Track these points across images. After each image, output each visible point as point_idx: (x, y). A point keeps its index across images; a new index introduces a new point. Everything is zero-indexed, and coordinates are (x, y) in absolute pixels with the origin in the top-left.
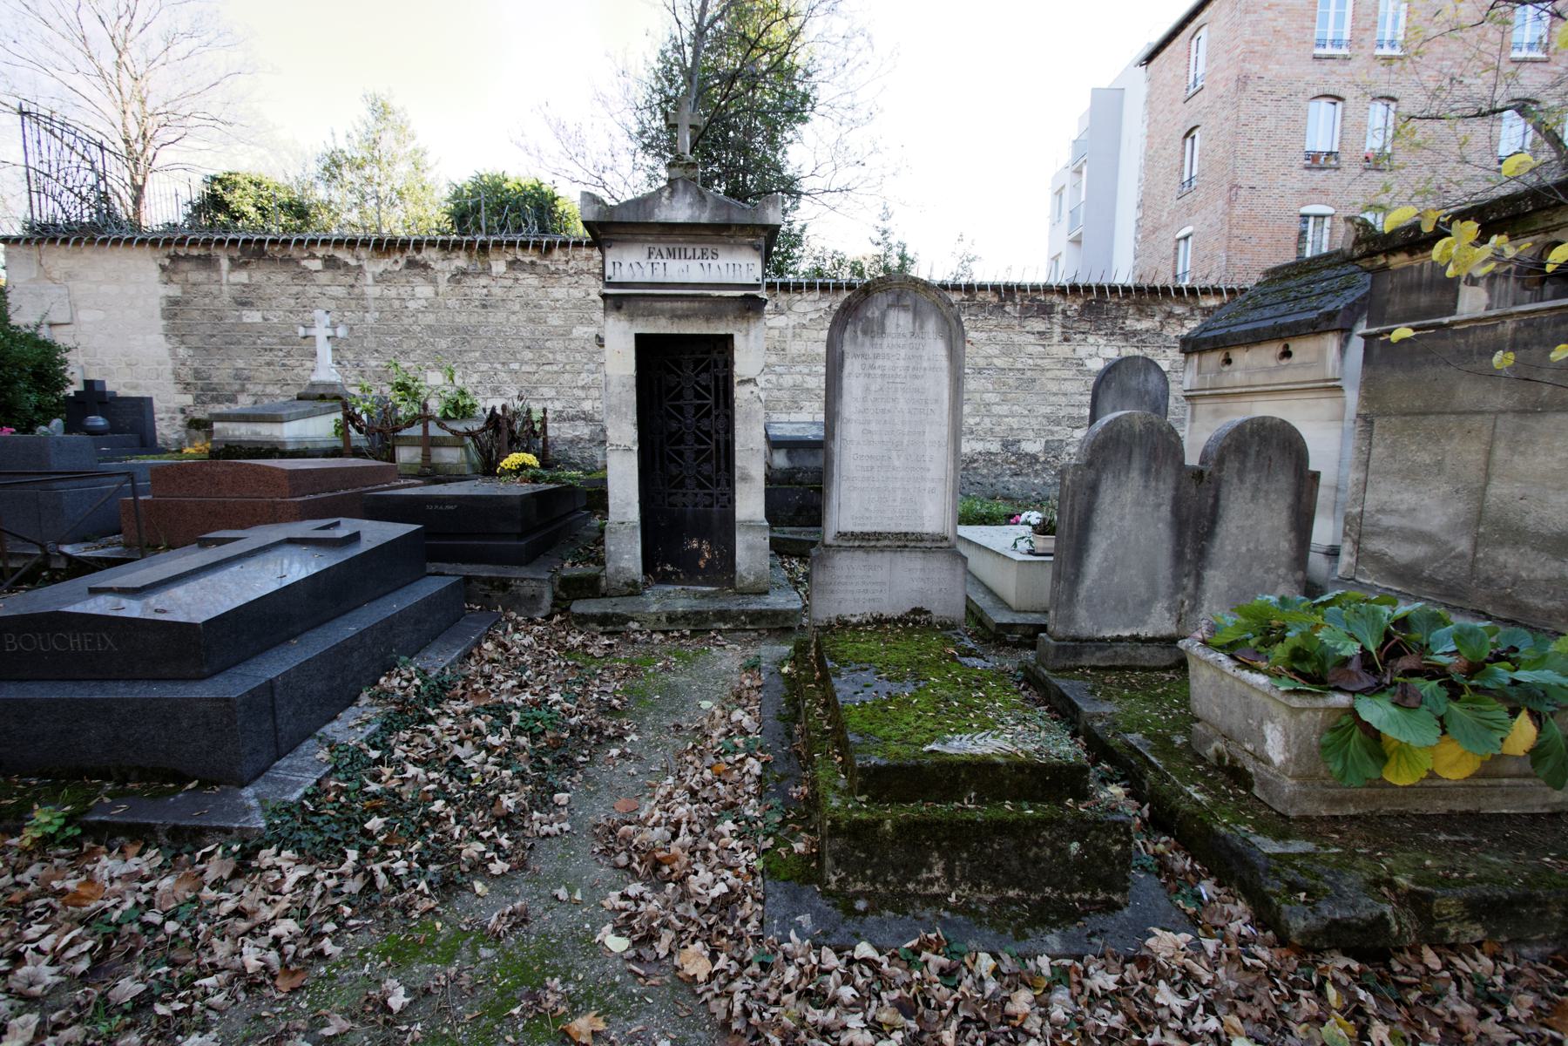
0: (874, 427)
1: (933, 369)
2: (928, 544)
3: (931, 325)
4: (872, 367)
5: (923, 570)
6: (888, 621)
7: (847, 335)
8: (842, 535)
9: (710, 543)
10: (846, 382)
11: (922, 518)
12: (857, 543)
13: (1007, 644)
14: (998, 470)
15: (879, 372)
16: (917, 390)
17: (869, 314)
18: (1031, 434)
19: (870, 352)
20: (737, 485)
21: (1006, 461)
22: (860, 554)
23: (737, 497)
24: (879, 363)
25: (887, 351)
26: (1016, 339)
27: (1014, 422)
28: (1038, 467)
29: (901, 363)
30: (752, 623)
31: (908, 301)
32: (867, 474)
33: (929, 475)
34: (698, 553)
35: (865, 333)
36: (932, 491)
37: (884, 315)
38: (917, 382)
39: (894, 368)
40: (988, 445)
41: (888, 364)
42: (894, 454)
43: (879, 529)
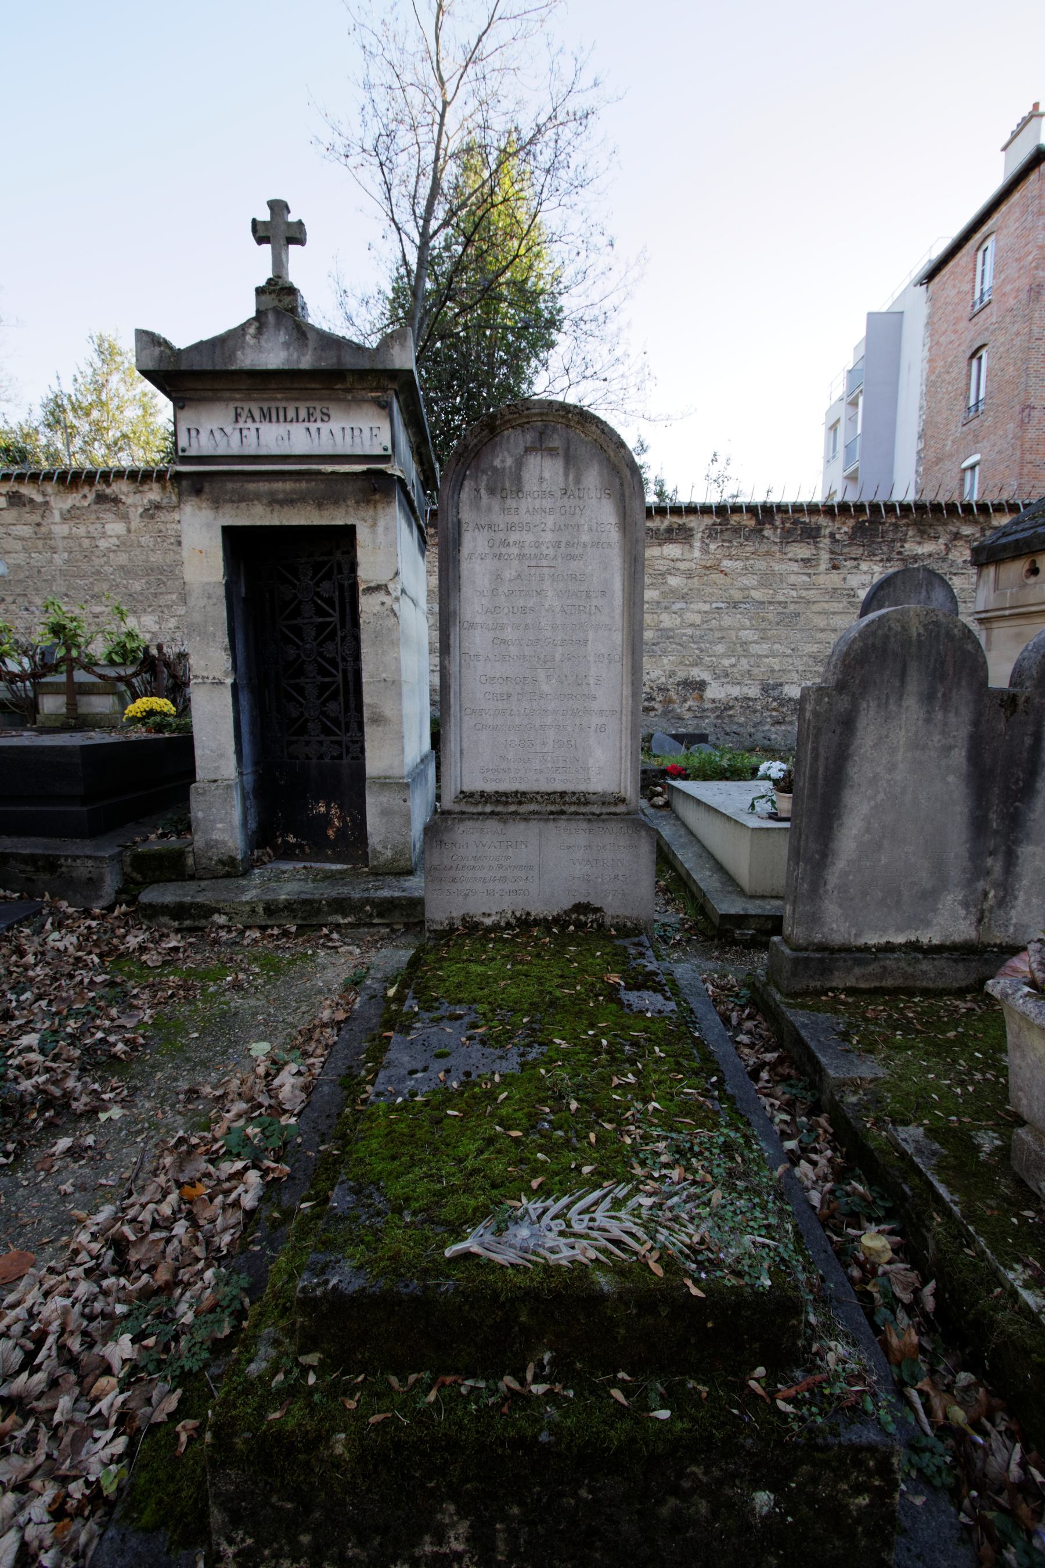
0: (509, 634)
1: (596, 545)
3: (593, 477)
4: (505, 543)
5: (589, 847)
6: (537, 922)
7: (465, 495)
8: (466, 796)
9: (340, 807)
10: (465, 567)
11: (586, 769)
12: (488, 809)
13: (735, 942)
14: (756, 717)
15: (514, 550)
16: (574, 578)
17: (497, 463)
18: (795, 677)
19: (500, 520)
20: (366, 729)
21: (766, 707)
22: (492, 824)
23: (367, 745)
24: (514, 537)
25: (526, 518)
26: (776, 567)
27: (775, 663)
29: (548, 537)
30: (380, 915)
31: (556, 442)
32: (500, 705)
33: (595, 706)
34: (325, 820)
35: (492, 491)
36: (601, 729)
37: (519, 464)
38: (574, 565)
39: (538, 545)
40: (745, 690)
41: (529, 538)
42: (541, 675)
43: (522, 787)
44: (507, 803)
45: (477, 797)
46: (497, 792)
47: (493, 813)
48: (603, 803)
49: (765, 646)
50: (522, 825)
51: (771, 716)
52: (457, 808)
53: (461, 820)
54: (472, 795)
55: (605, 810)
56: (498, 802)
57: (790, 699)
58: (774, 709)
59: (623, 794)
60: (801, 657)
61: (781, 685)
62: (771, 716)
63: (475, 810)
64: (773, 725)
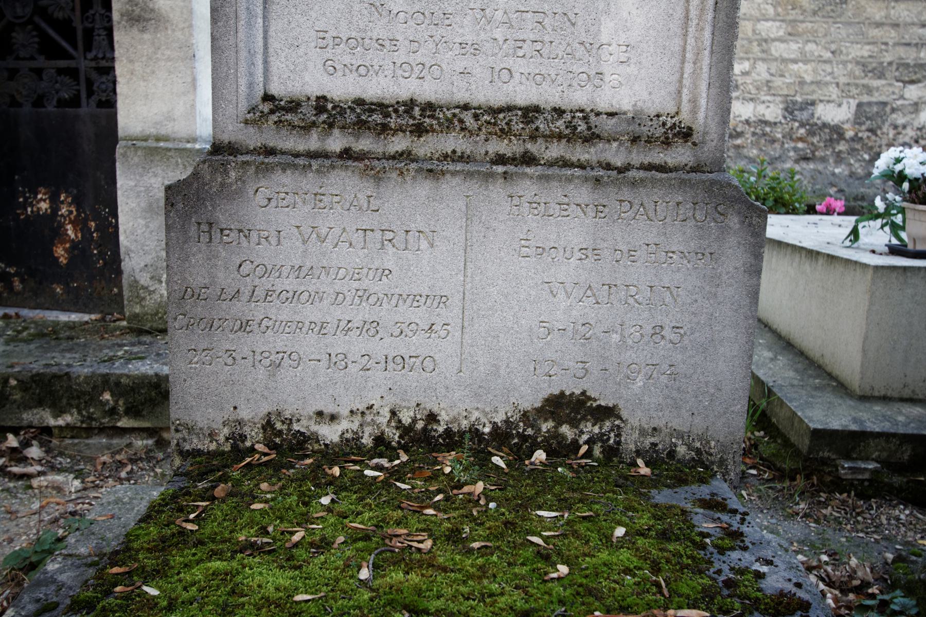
2: (615, 154)
5: (591, 252)
6: (452, 440)
9: (78, 202)
11: (592, 47)
12: (336, 143)
13: (839, 485)
14: (774, 151)
18: (834, 92)
20: (117, 36)
21: (789, 136)
22: (345, 183)
23: (120, 69)
27: (806, 71)
28: (842, 147)
30: (133, 411)
34: (50, 227)
40: (761, 109)
43: (427, 90)
44: (384, 129)
45: (308, 111)
46: (360, 102)
47: (347, 154)
48: (635, 140)
49: (794, 46)
50: (423, 189)
51: (795, 149)
52: (252, 138)
53: (264, 170)
54: (294, 105)
55: (638, 157)
56: (361, 125)
57: (825, 125)
58: (801, 139)
59: (685, 117)
60: (844, 63)
61: (813, 103)
62: (795, 149)
63: (301, 147)
64: (797, 161)
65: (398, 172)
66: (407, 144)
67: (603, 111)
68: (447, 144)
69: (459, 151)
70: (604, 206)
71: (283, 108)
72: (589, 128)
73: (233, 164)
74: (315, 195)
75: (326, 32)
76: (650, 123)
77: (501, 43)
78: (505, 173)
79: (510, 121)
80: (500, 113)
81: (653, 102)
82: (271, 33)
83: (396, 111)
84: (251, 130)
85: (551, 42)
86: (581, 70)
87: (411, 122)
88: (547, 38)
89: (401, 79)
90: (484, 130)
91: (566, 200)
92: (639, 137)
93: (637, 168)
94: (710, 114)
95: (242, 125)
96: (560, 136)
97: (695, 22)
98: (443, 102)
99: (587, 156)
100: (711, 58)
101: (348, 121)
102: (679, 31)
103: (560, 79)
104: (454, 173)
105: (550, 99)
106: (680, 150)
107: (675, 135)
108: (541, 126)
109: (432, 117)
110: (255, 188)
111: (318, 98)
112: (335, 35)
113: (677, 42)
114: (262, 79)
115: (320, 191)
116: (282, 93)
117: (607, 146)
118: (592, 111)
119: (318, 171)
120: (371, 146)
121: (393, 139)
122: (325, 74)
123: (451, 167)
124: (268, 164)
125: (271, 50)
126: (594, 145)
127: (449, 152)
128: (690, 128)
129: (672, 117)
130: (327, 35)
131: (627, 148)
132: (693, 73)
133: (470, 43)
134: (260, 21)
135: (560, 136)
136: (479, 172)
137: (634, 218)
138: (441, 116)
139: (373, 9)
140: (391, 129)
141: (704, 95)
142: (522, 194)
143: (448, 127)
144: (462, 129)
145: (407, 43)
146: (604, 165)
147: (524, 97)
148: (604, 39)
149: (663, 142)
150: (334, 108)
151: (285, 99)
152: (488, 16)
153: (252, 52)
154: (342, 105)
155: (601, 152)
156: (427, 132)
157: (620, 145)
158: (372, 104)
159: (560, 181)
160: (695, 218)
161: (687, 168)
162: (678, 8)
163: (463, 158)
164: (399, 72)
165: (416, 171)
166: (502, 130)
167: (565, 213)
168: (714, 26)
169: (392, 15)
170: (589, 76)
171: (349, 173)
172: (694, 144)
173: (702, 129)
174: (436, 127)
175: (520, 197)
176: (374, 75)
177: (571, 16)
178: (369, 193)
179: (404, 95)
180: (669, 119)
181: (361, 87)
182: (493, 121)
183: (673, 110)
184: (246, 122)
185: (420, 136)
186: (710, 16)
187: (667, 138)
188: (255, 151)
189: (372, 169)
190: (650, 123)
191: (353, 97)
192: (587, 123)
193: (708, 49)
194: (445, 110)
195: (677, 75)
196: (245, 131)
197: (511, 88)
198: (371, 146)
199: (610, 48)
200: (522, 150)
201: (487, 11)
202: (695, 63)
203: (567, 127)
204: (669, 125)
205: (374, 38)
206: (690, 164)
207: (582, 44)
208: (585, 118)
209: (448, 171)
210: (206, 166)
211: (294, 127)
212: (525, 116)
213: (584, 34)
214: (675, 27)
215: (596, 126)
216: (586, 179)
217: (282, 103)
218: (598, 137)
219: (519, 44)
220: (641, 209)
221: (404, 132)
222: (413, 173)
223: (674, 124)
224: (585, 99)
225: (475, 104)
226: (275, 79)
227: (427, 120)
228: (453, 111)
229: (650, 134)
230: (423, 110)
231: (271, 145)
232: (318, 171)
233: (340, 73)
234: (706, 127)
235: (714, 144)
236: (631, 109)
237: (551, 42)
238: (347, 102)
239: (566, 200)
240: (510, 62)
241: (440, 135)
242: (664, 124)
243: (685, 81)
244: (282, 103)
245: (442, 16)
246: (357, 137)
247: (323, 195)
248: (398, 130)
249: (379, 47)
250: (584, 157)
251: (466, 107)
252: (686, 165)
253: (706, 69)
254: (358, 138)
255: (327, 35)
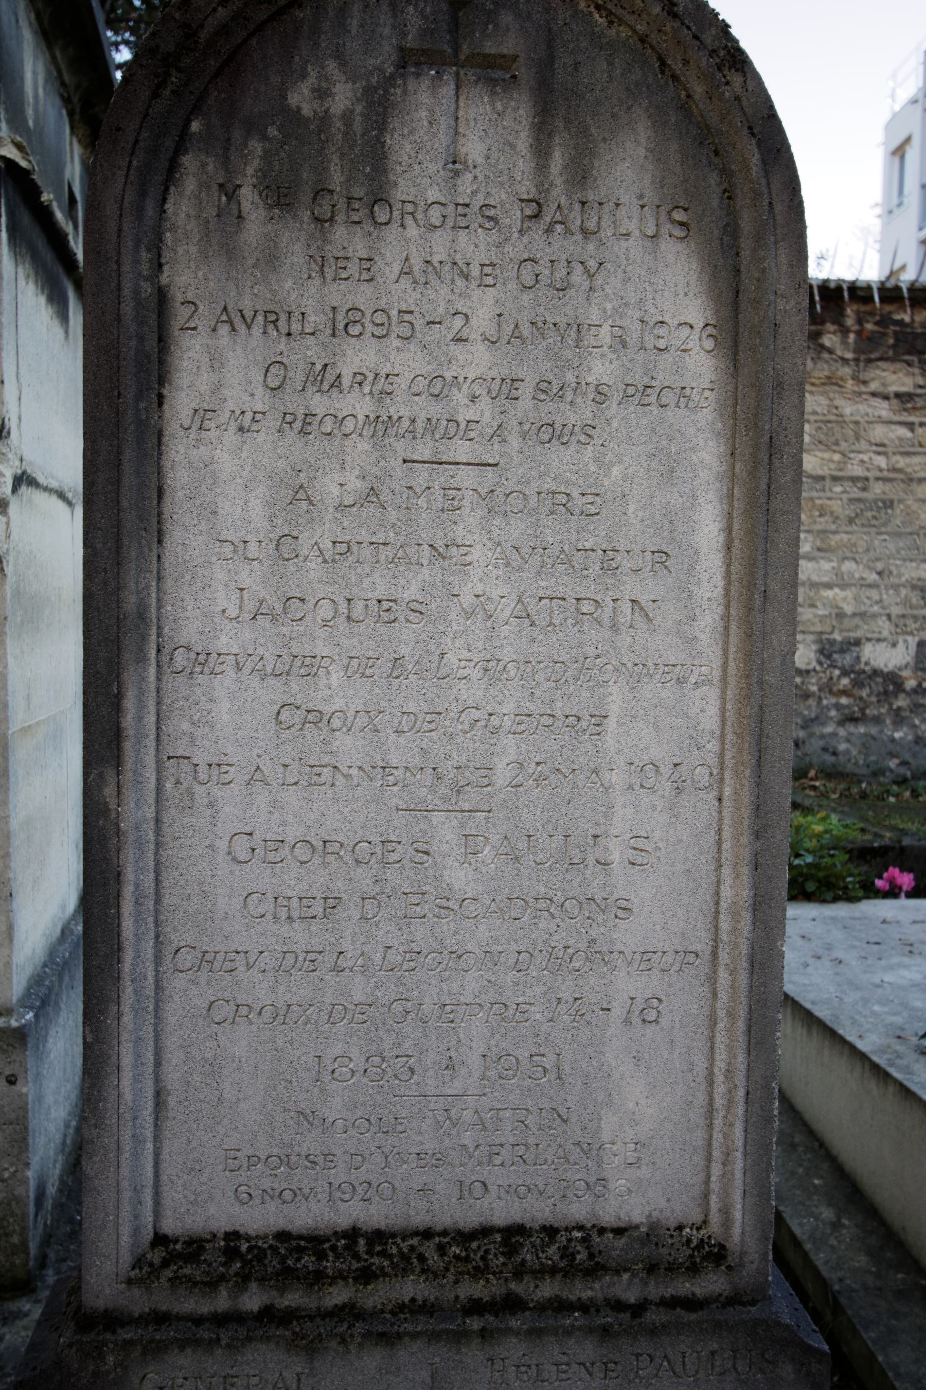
0: (335, 691)
1: (641, 393)
2: (627, 1289)
3: (629, 169)
4: (324, 379)
7: (182, 207)
8: (174, 1255)
10: (182, 457)
11: (592, 1150)
12: (252, 1300)
14: (809, 709)
15: (359, 405)
16: (560, 504)
17: (301, 98)
18: (885, 628)
19: (311, 298)
21: (828, 688)
24: (356, 357)
25: (402, 295)
26: (848, 409)
27: (845, 599)
28: (901, 702)
29: (477, 361)
31: (508, 40)
32: (301, 937)
33: (628, 936)
35: (280, 197)
36: (645, 1014)
37: (380, 107)
38: (560, 459)
39: (438, 387)
41: (408, 363)
42: (445, 831)
44: (318, 1278)
45: (213, 1255)
46: (283, 1236)
47: (267, 1314)
48: (651, 1268)
49: (826, 566)
50: (372, 1360)
51: (838, 706)
52: (138, 1302)
53: (155, 1350)
54: (194, 1247)
55: (656, 1290)
56: (287, 1276)
57: (876, 672)
58: (844, 693)
59: (715, 1226)
60: (896, 587)
61: (857, 643)
62: (838, 706)
63: (205, 1308)
64: (841, 723)
65: (339, 1339)
66: (349, 1295)
67: (608, 1225)
68: (404, 1292)
69: (419, 1298)
70: (616, 1363)
71: (180, 1256)
72: (591, 1256)
73: (111, 1346)
74: (225, 1377)
75: (238, 1150)
76: (670, 1241)
77: (471, 1150)
78: (483, 1329)
79: (487, 1252)
80: (473, 1240)
81: (673, 1211)
82: (165, 1155)
83: (334, 1248)
84: (136, 1292)
85: (537, 1145)
86: (577, 1177)
87: (355, 1265)
88: (531, 1141)
89: (339, 1203)
90: (452, 1270)
91: (565, 1359)
92: (657, 1264)
93: (656, 1304)
94: (747, 1229)
95: (124, 1286)
96: (553, 1271)
97: (722, 1113)
98: (396, 1228)
99: (590, 1293)
100: (745, 1160)
101: (270, 1270)
102: (702, 1122)
103: (550, 1190)
104: (415, 1336)
105: (539, 1215)
106: (713, 1277)
107: (703, 1259)
108: (528, 1257)
109: (383, 1254)
110: (141, 1375)
111: (227, 1234)
112: (250, 1153)
113: (699, 1136)
114: (151, 1219)
115: (231, 1372)
116: (179, 1232)
117: (616, 1278)
118: (594, 1226)
119: (228, 1346)
120: (301, 1300)
121: (331, 1290)
122: (237, 1204)
123: (409, 1327)
124: (160, 1341)
125: (164, 1178)
126: (599, 1278)
127: (406, 1301)
128: (722, 1247)
129: (698, 1229)
130: (239, 1154)
131: (641, 1280)
132: (723, 1175)
133: (430, 1152)
134: (150, 1146)
135: (553, 1271)
136: (447, 1331)
137: (657, 1375)
138: (394, 1250)
139: (302, 1118)
140: (328, 1277)
141: (739, 1206)
142: (507, 1354)
143: (403, 1269)
144: (423, 1271)
145: (347, 1158)
146: (613, 1302)
147: (504, 1215)
148: (606, 1136)
149: (687, 1269)
150: (250, 1249)
151: (182, 1239)
152: (454, 1117)
153: (139, 1187)
154: (260, 1243)
155: (608, 1287)
156: (376, 1277)
157: (634, 1275)
158: (300, 1237)
159: (556, 1335)
160: (735, 1369)
161: (722, 1299)
162: (699, 1094)
163: (425, 1309)
164: (338, 1194)
165: (363, 1336)
166: (476, 1268)
167: (564, 1376)
168: (746, 1121)
169: (326, 1125)
170: (587, 1184)
171: (272, 1346)
172: (729, 1268)
173: (738, 1249)
174: (388, 1270)
175: (503, 1359)
176: (303, 1201)
177: (563, 1112)
178: (299, 1370)
179: (343, 1222)
180: (695, 1232)
181: (285, 1217)
182: (464, 1254)
183: (697, 1218)
184: (130, 1282)
185: (366, 1283)
186: (740, 1110)
187: (694, 1264)
188: (143, 1320)
189: (303, 1338)
190: (670, 1241)
191: (275, 1230)
192: (587, 1248)
193: (741, 1150)
194: (399, 1240)
195: (702, 1175)
196: (128, 1294)
197: (486, 1205)
198: (301, 1300)
199: (615, 1148)
200: (503, 1290)
201: (453, 1112)
202: (724, 1164)
203: (562, 1258)
204: (695, 1242)
205: (303, 1153)
206: (726, 1293)
207: (578, 1144)
208: (584, 1240)
209: (406, 1334)
210: (74, 1349)
211: (196, 1284)
212: (505, 1242)
213: (579, 1133)
214: (697, 1115)
215: (600, 1252)
216: (590, 1330)
217: (178, 1247)
218: (604, 1268)
219: (496, 1149)
220: (665, 1363)
221: (344, 1278)
222: (359, 1340)
223: (702, 1240)
224: (584, 1212)
225: (439, 1228)
226: (169, 1213)
227: (376, 1260)
228: (411, 1242)
229: (671, 1259)
230: (370, 1244)
231: (164, 1308)
232: (228, 1346)
233: (257, 1201)
234: (742, 1245)
235: (754, 1266)
236: (644, 1221)
237: (537, 1145)
238: (266, 1236)
239: (565, 1359)
240: (484, 1173)
241: (394, 1280)
242: (689, 1241)
243: (712, 1186)
244: (178, 1247)
245: (393, 1121)
246: (282, 1291)
247: (237, 1377)
248: (336, 1278)
249: (309, 1164)
250: (587, 1294)
251: (427, 1234)
252: (720, 1295)
253: (739, 1175)
254: (283, 1292)
255: (239, 1154)
